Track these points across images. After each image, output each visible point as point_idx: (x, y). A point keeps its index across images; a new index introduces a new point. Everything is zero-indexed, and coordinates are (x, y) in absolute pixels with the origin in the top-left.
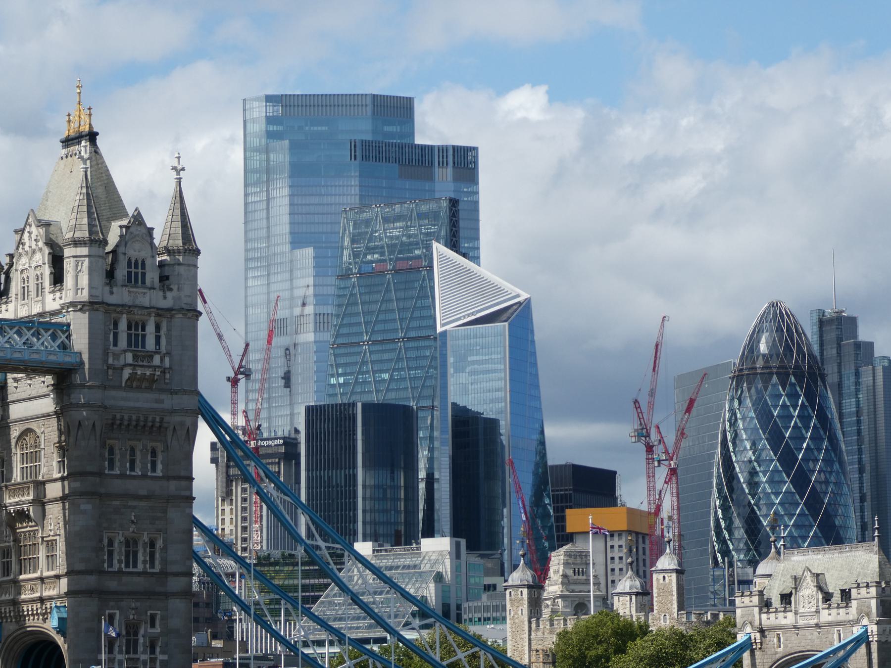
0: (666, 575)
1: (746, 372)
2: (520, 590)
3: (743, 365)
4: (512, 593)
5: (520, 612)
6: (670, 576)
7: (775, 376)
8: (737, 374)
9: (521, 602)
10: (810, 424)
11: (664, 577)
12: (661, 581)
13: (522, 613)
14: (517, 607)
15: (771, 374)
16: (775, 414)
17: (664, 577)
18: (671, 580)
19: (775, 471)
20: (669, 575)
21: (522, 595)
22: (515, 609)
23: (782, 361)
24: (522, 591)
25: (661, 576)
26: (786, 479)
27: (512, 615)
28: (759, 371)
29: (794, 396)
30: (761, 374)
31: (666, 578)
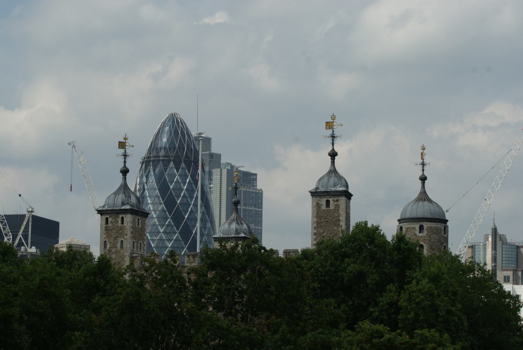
0: (331, 200)
1: (152, 159)
2: (121, 216)
3: (150, 154)
4: (110, 220)
5: (119, 245)
6: (337, 201)
7: (172, 163)
8: (145, 160)
9: (121, 231)
10: (193, 194)
11: (328, 202)
12: (324, 207)
13: (122, 247)
14: (116, 238)
15: (169, 161)
16: (171, 188)
17: (328, 202)
18: (337, 206)
19: (169, 225)
20: (336, 199)
21: (123, 223)
22: (112, 240)
23: (177, 152)
24: (123, 218)
25: (323, 201)
26: (176, 231)
27: (108, 248)
28: (161, 158)
29: (184, 177)
30: (163, 160)
31: (332, 203)
